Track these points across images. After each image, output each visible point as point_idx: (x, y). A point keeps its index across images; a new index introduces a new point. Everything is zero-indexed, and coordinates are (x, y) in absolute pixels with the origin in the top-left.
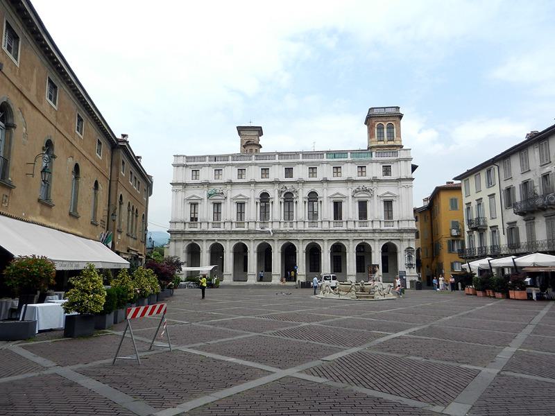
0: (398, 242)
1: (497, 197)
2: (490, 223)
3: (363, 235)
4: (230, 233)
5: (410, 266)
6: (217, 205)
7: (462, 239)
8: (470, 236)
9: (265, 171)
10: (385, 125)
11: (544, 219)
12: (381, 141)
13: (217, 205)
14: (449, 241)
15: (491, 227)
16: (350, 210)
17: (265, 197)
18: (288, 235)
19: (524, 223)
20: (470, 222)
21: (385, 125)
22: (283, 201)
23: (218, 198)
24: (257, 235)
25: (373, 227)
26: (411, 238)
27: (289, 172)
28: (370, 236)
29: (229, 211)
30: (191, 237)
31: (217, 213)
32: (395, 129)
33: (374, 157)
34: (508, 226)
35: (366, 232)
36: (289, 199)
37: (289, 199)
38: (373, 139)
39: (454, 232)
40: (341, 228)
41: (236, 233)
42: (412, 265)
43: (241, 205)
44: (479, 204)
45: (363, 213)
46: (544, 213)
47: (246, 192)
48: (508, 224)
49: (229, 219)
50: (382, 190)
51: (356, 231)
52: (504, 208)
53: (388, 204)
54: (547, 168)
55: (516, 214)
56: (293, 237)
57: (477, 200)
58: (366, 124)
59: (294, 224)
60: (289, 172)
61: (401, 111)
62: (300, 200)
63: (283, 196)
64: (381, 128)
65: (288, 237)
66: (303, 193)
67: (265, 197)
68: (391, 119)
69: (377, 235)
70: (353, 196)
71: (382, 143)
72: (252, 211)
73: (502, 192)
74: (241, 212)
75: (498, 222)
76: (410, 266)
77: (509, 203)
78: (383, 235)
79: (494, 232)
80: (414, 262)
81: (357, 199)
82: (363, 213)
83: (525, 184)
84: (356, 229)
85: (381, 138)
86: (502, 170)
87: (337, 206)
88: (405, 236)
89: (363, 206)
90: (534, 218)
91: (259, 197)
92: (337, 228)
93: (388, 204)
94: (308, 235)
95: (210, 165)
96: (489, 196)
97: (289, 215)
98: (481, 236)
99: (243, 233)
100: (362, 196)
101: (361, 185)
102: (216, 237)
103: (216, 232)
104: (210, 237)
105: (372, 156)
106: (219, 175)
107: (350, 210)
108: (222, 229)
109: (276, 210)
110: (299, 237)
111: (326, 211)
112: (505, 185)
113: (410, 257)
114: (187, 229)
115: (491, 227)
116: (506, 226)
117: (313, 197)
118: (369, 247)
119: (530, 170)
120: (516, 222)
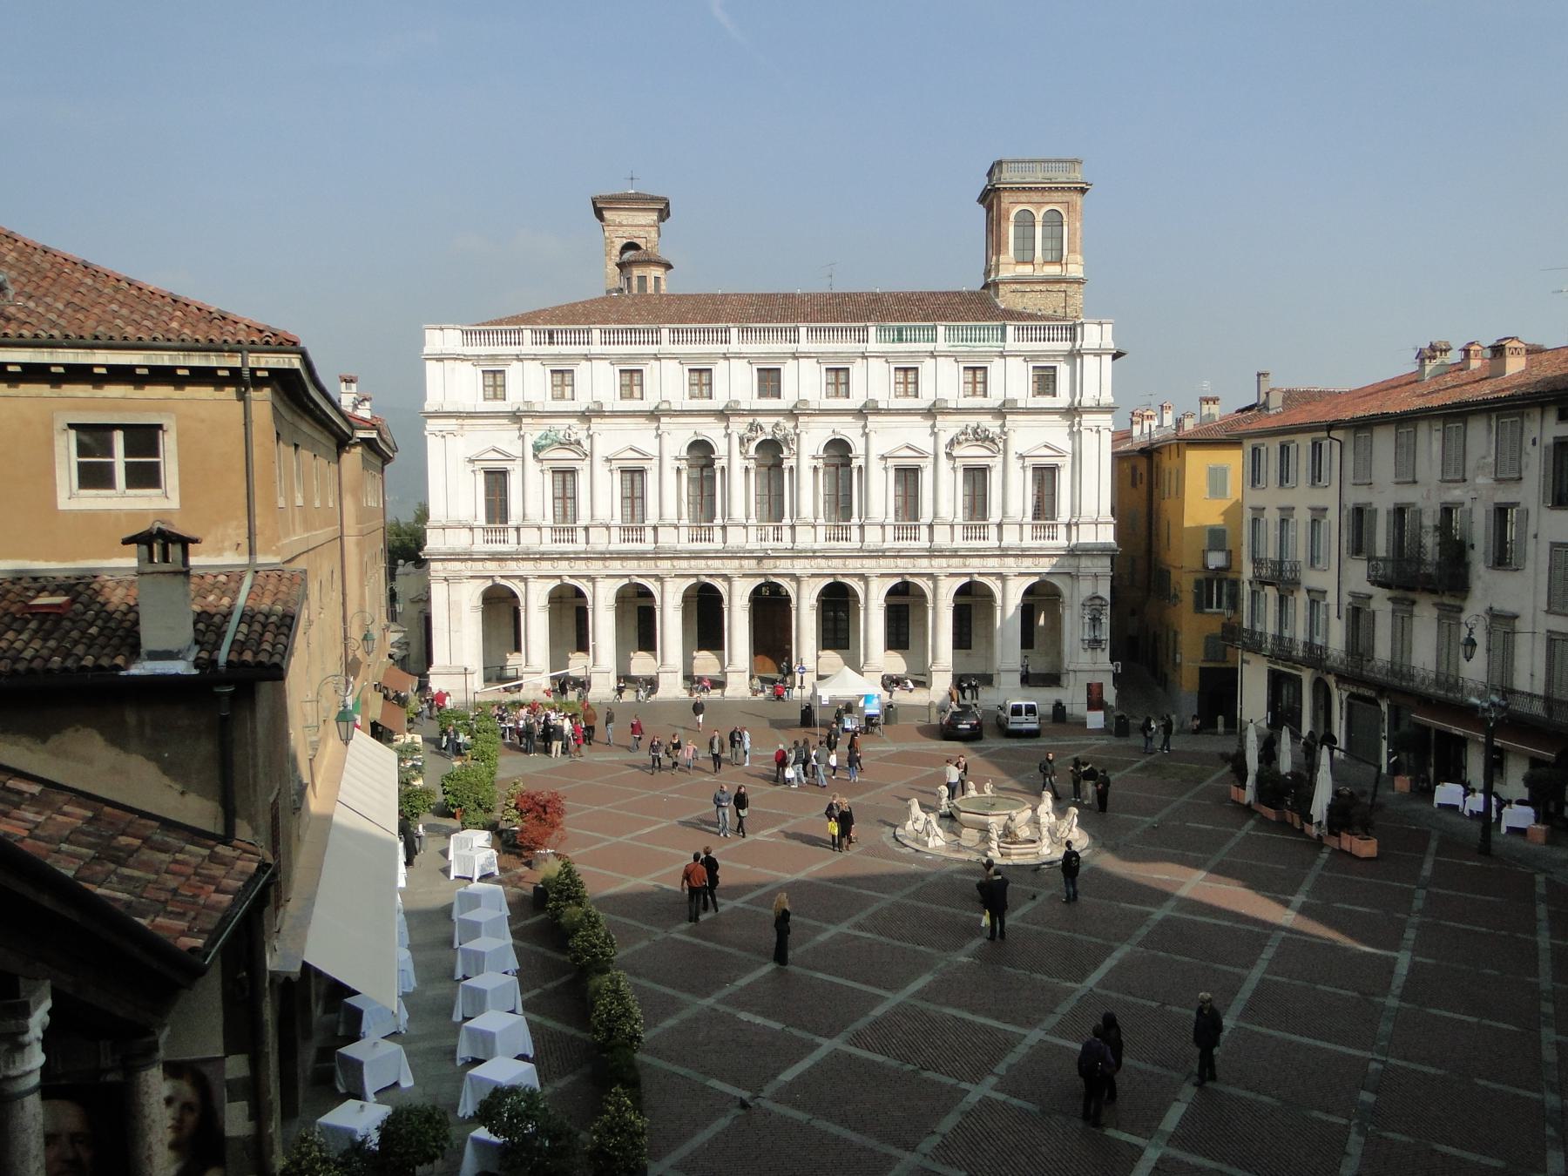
0: (1067, 580)
1: (1332, 515)
2: (1311, 579)
3: (976, 562)
4: (604, 557)
5: (1095, 643)
6: (565, 475)
7: (1231, 576)
8: (1254, 593)
10: (1039, 217)
11: (1435, 612)
12: (1024, 263)
13: (565, 475)
15: (1309, 591)
17: (701, 451)
18: (768, 563)
19: (1390, 606)
20: (1257, 562)
21: (1039, 217)
22: (752, 464)
23: (564, 457)
24: (684, 564)
25: (1000, 539)
27: (769, 381)
28: (993, 564)
30: (491, 568)
32: (1065, 228)
33: (1011, 344)
34: (1350, 600)
35: (981, 555)
36: (771, 454)
37: (771, 454)
39: (1216, 560)
40: (913, 544)
41: (623, 556)
42: (1099, 642)
43: (633, 475)
45: (977, 504)
46: (1436, 599)
47: (641, 436)
49: (602, 513)
51: (955, 554)
52: (1344, 552)
53: (1045, 476)
55: (1373, 584)
56: (784, 566)
59: (787, 533)
60: (769, 381)
62: (806, 465)
63: (752, 451)
64: (1025, 221)
65: (769, 567)
66: (812, 440)
67: (701, 451)
68: (1057, 196)
69: (1010, 561)
70: (949, 455)
71: (1026, 270)
73: (1345, 513)
74: (634, 498)
76: (1095, 643)
77: (1359, 544)
78: (1028, 562)
79: (1313, 603)
80: (1105, 634)
81: (959, 462)
82: (977, 504)
83: (1399, 512)
84: (955, 546)
87: (908, 477)
89: (976, 476)
90: (1413, 603)
91: (684, 453)
93: (1045, 476)
94: (823, 562)
95: (535, 358)
98: (1282, 601)
99: (640, 556)
101: (972, 421)
102: (563, 568)
103: (563, 557)
104: (546, 567)
105: (1004, 339)
106: (563, 384)
108: (580, 546)
110: (799, 567)
111: (880, 493)
113: (1095, 621)
114: (480, 546)
115: (1309, 591)
116: (1346, 599)
117: (839, 450)
118: (988, 595)
119: (1415, 482)
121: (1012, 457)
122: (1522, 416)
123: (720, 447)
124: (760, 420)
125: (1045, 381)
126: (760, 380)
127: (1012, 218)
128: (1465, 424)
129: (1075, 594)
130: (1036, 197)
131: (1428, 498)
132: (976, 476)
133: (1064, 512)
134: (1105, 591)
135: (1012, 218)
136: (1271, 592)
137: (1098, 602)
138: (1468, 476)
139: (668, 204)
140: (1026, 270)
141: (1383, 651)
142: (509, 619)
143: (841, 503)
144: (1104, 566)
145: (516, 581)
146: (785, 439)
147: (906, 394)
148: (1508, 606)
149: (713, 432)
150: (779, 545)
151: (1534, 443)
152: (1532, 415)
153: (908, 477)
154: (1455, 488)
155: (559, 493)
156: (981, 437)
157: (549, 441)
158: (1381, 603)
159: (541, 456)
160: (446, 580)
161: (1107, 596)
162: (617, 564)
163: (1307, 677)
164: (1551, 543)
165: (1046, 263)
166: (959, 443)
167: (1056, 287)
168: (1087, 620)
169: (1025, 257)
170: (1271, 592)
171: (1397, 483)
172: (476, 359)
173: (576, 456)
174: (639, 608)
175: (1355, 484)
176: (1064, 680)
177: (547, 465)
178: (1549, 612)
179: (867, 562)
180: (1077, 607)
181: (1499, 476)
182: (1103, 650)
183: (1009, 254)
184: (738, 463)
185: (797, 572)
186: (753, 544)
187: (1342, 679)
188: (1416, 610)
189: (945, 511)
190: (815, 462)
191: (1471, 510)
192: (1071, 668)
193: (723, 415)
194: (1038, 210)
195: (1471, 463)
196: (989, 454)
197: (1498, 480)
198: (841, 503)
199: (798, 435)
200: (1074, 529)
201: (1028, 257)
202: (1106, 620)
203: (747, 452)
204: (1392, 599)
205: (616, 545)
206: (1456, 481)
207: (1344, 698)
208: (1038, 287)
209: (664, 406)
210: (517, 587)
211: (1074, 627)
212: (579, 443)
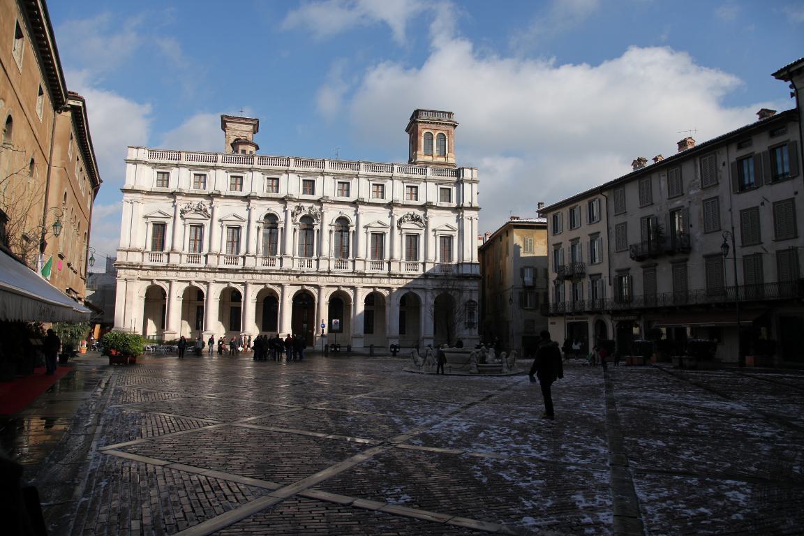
1: (604, 235)
5: (470, 325)
8: (557, 287)
10: (435, 136)
14: (520, 293)
17: (271, 219)
22: (297, 227)
27: (309, 186)
29: (218, 239)
30: (152, 274)
31: (197, 240)
32: (447, 142)
34: (617, 274)
36: (308, 225)
42: (474, 324)
44: (573, 247)
48: (617, 271)
54: (678, 202)
55: (633, 259)
57: (571, 240)
58: (407, 130)
60: (309, 186)
61: (455, 118)
62: (326, 229)
63: (298, 220)
64: (429, 137)
65: (303, 280)
67: (271, 219)
69: (429, 282)
70: (399, 228)
71: (429, 159)
72: (254, 240)
75: (602, 269)
84: (402, 273)
85: (429, 152)
86: (612, 203)
87: (378, 238)
89: (413, 240)
90: (656, 265)
91: (262, 219)
92: (376, 271)
96: (589, 235)
97: (308, 249)
99: (236, 271)
101: (411, 211)
102: (192, 276)
103: (193, 270)
104: (182, 275)
109: (292, 240)
111: (364, 245)
112: (615, 221)
114: (147, 262)
116: (614, 274)
117: (343, 222)
119: (652, 204)
120: (629, 269)
122: (715, 153)
123: (281, 217)
124: (303, 204)
125: (446, 194)
126: (304, 185)
127: (423, 135)
128: (681, 167)
130: (434, 126)
131: (661, 210)
132: (413, 240)
134: (475, 298)
135: (423, 135)
136: (568, 284)
137: (472, 303)
138: (684, 192)
139: (258, 122)
141: (639, 292)
142: (160, 312)
144: (474, 285)
146: (316, 215)
147: (378, 197)
150: (310, 269)
151: (724, 164)
152: (720, 152)
154: (677, 201)
155: (193, 237)
156: (415, 219)
157: (190, 209)
158: (637, 270)
159: (185, 216)
160: (126, 280)
163: (591, 321)
164: (741, 211)
165: (438, 156)
166: (404, 221)
169: (429, 152)
170: (568, 284)
171: (640, 208)
172: (155, 165)
173: (202, 217)
174: (232, 307)
175: (615, 215)
177: (188, 221)
179: (356, 280)
181: (704, 186)
182: (475, 328)
183: (421, 152)
184: (290, 226)
185: (319, 284)
187: (614, 313)
188: (658, 268)
189: (397, 255)
190: (330, 228)
191: (688, 208)
193: (283, 201)
195: (686, 185)
196: (418, 228)
197: (703, 189)
198: (343, 252)
199: (322, 213)
200: (460, 266)
202: (476, 313)
203: (295, 220)
204: (643, 267)
205: (222, 265)
206: (678, 197)
207: (615, 325)
209: (252, 194)
211: (460, 316)
212: (206, 211)
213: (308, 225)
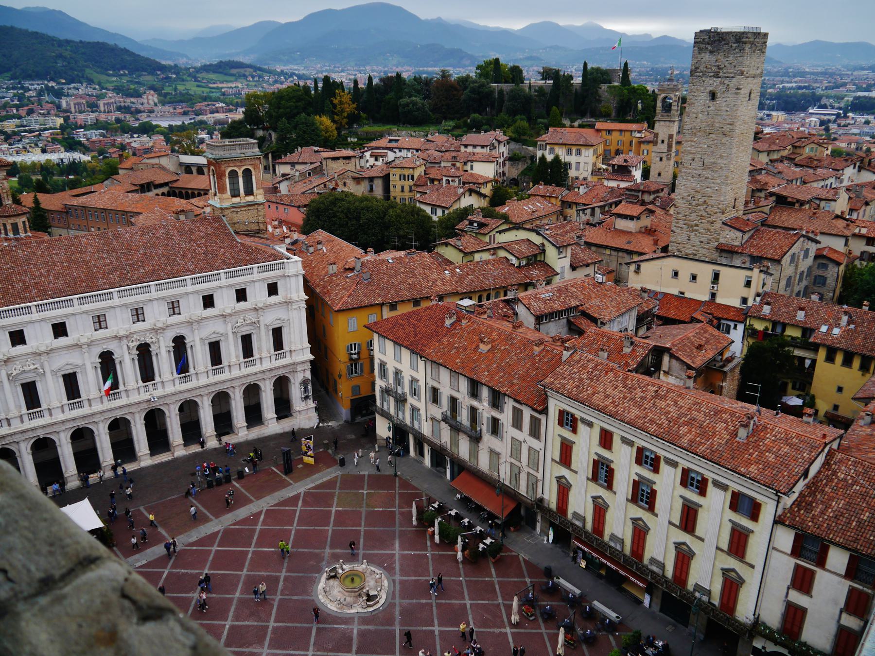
9: (100, 321)
16: (231, 351)
22: (136, 357)
26: (305, 368)
32: (254, 178)
38: (225, 196)
50: (270, 319)
59: (159, 386)
64: (233, 175)
68: (248, 162)
69: (267, 373)
87: (215, 349)
88: (300, 368)
93: (277, 333)
97: (147, 373)
100: (245, 331)
107: (231, 351)
113: (306, 390)
121: (263, 328)
129: (296, 379)
133: (286, 347)
134: (308, 375)
140: (237, 200)
143: (182, 365)
144: (308, 366)
145: (13, 445)
148: (498, 450)
149: (112, 346)
153: (215, 349)
161: (310, 378)
162: (72, 422)
167: (253, 207)
168: (303, 390)
176: (295, 414)
178: (511, 456)
180: (297, 385)
185: (168, 402)
186: (145, 396)
192: (298, 409)
193: (116, 338)
194: (239, 169)
198: (182, 365)
199: (158, 339)
201: (236, 193)
202: (310, 387)
208: (243, 209)
210: (13, 448)
211: (296, 392)
213: (144, 353)
